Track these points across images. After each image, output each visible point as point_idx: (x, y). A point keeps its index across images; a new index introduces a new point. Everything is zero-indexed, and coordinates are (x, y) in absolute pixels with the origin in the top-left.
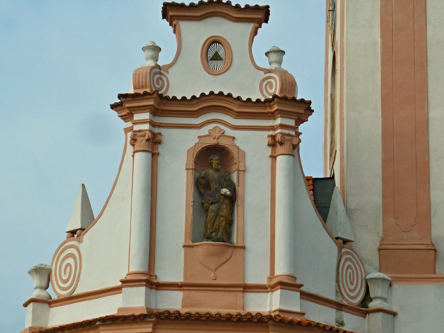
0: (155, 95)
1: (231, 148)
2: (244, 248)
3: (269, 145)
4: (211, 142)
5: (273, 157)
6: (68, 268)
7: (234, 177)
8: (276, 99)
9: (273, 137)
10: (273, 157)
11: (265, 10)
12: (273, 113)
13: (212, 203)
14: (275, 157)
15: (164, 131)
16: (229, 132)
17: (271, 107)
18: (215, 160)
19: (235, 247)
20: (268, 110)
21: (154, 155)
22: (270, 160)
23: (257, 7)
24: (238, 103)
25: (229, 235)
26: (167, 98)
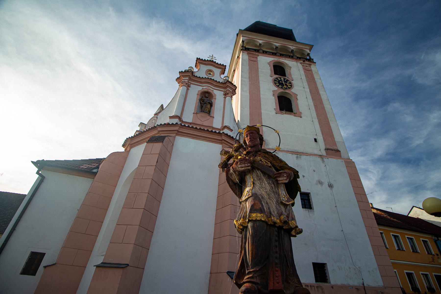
0: (191, 72)
1: (213, 94)
2: (214, 117)
3: (224, 95)
4: (206, 90)
5: (225, 98)
6: (152, 123)
7: (213, 101)
8: (228, 82)
9: (225, 93)
10: (225, 98)
11: (225, 66)
12: (225, 87)
13: (205, 104)
14: (226, 98)
15: (192, 85)
16: (211, 89)
17: (225, 85)
18: (207, 95)
19: (211, 117)
20: (225, 86)
21: (188, 89)
22: (223, 99)
23: (223, 65)
24: (216, 82)
25: (209, 113)
26: (194, 76)
